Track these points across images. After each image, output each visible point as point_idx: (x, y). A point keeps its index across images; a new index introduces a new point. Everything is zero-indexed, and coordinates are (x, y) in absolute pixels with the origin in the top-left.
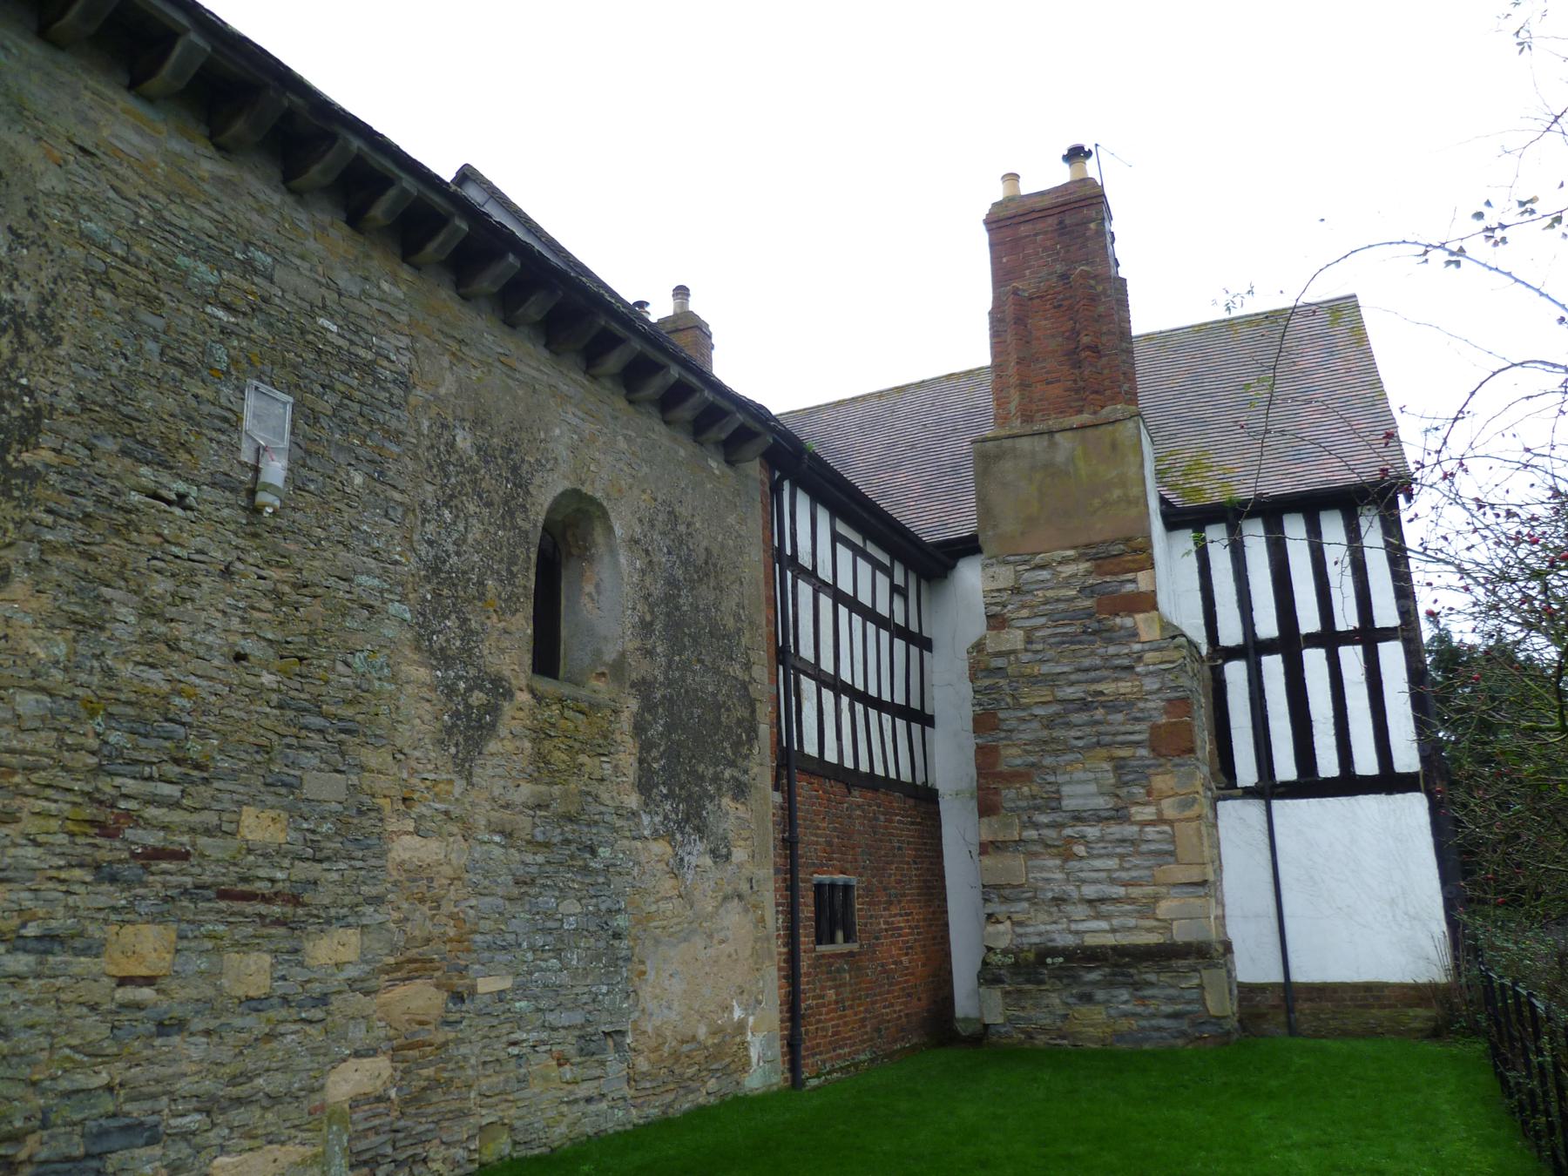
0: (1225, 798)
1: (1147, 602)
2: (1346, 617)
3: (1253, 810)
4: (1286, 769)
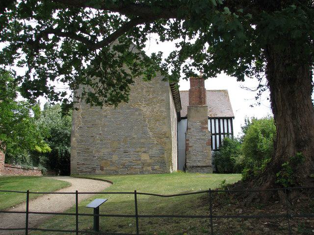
1: (207, 128)
2: (226, 132)
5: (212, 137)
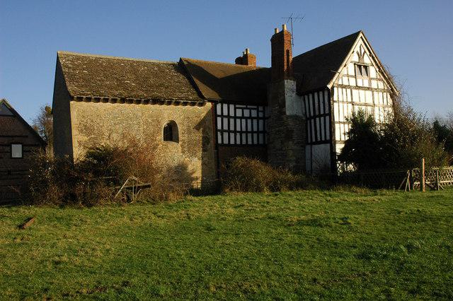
2: (322, 113)
4: (314, 140)
5: (307, 124)
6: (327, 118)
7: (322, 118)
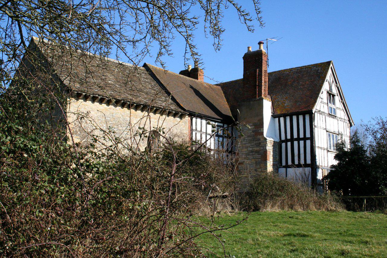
0: (280, 168)
2: (302, 136)
3: (284, 169)
4: (290, 163)
6: (308, 142)
7: (302, 142)
